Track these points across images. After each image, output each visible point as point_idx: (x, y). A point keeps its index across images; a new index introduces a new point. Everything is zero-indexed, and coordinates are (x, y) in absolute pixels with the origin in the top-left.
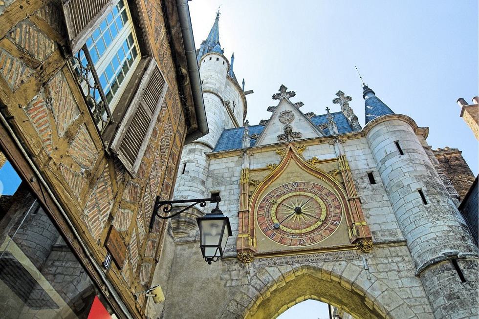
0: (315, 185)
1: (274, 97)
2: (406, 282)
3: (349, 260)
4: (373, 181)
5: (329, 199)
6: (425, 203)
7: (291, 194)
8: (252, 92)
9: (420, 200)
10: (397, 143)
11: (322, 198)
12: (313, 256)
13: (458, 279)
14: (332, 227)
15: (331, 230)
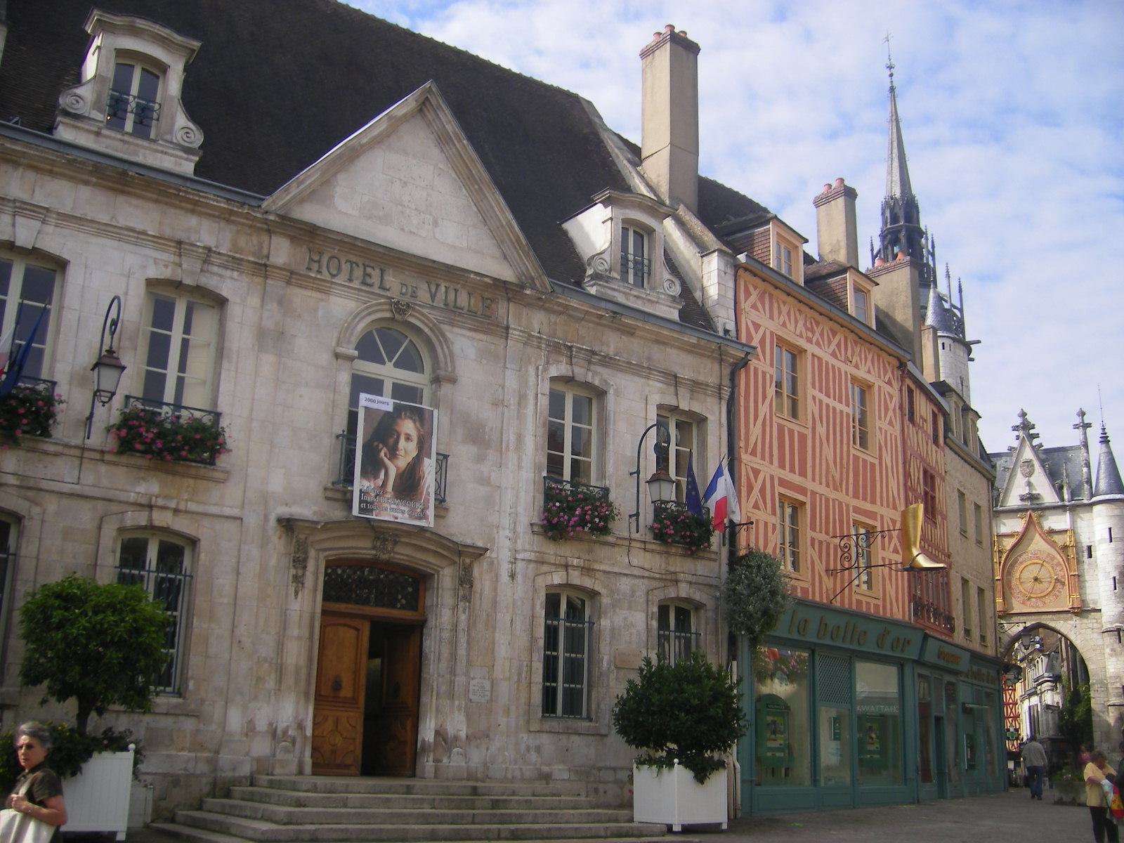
0: (1049, 554)
1: (1015, 428)
2: (1095, 636)
3: (1065, 620)
4: (1090, 556)
5: (1058, 569)
6: (1115, 589)
7: (1030, 562)
8: (979, 342)
9: (1113, 586)
10: (1110, 529)
11: (1053, 568)
12: (1044, 617)
13: (1118, 641)
14: (1058, 594)
15: (1057, 596)
